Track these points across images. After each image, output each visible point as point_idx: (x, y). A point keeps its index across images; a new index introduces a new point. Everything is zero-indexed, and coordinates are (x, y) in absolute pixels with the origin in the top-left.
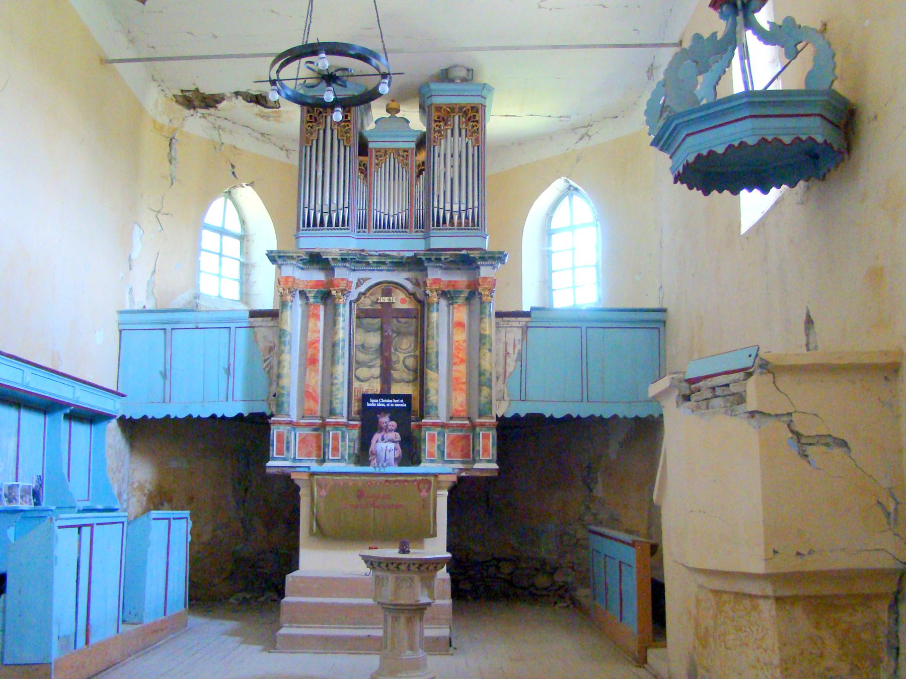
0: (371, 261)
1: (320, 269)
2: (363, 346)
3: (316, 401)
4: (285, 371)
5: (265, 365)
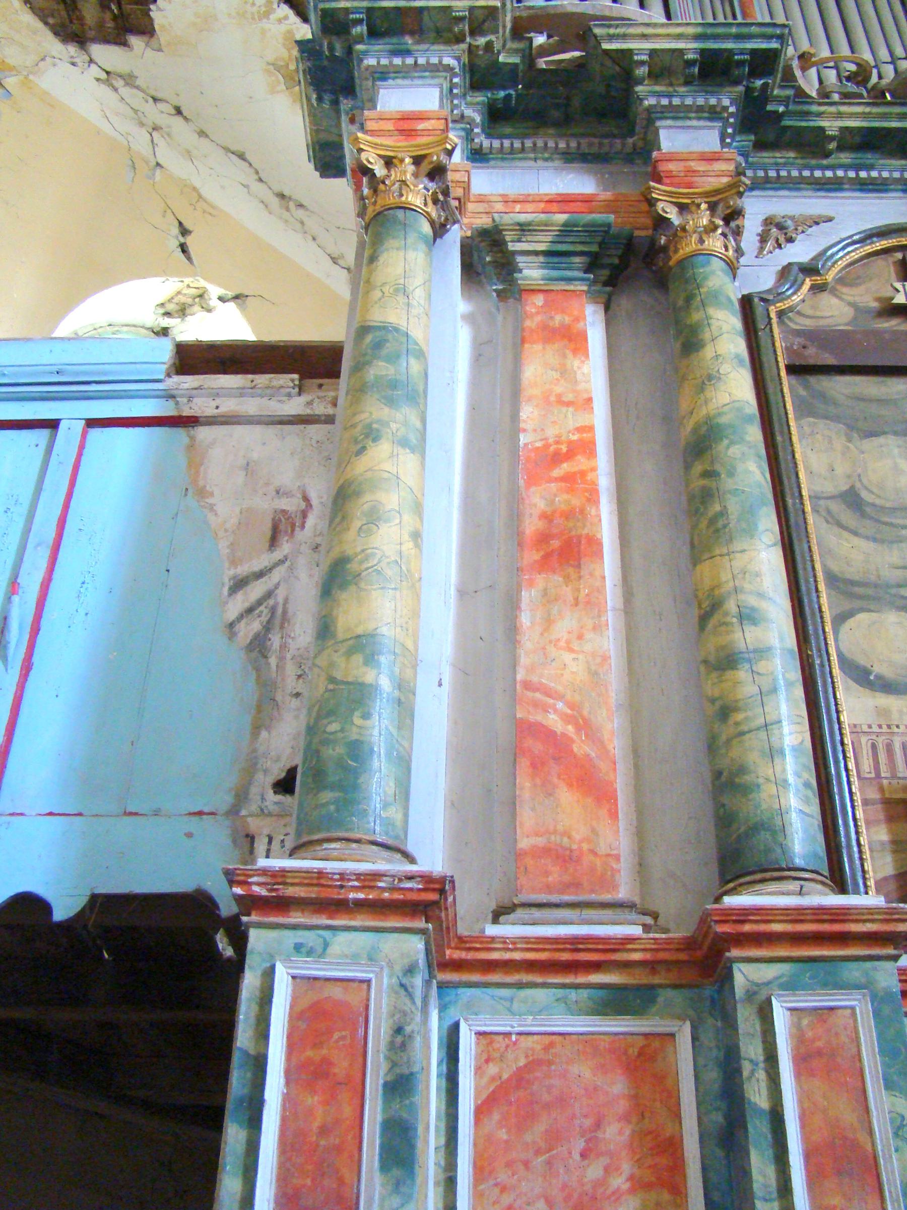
0: (832, 126)
1: (571, 158)
2: (852, 499)
3: (590, 784)
4: (387, 541)
5: (237, 605)
